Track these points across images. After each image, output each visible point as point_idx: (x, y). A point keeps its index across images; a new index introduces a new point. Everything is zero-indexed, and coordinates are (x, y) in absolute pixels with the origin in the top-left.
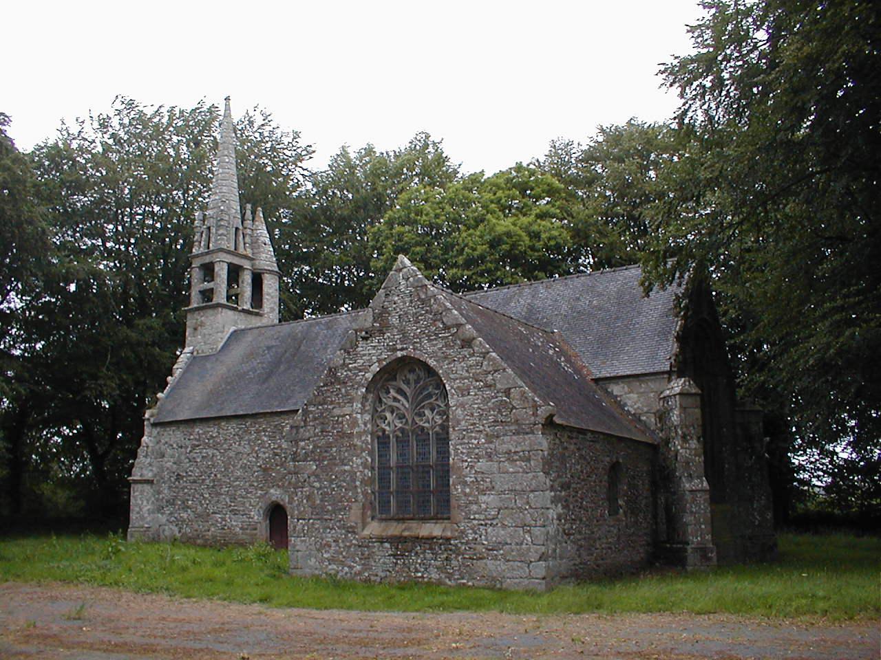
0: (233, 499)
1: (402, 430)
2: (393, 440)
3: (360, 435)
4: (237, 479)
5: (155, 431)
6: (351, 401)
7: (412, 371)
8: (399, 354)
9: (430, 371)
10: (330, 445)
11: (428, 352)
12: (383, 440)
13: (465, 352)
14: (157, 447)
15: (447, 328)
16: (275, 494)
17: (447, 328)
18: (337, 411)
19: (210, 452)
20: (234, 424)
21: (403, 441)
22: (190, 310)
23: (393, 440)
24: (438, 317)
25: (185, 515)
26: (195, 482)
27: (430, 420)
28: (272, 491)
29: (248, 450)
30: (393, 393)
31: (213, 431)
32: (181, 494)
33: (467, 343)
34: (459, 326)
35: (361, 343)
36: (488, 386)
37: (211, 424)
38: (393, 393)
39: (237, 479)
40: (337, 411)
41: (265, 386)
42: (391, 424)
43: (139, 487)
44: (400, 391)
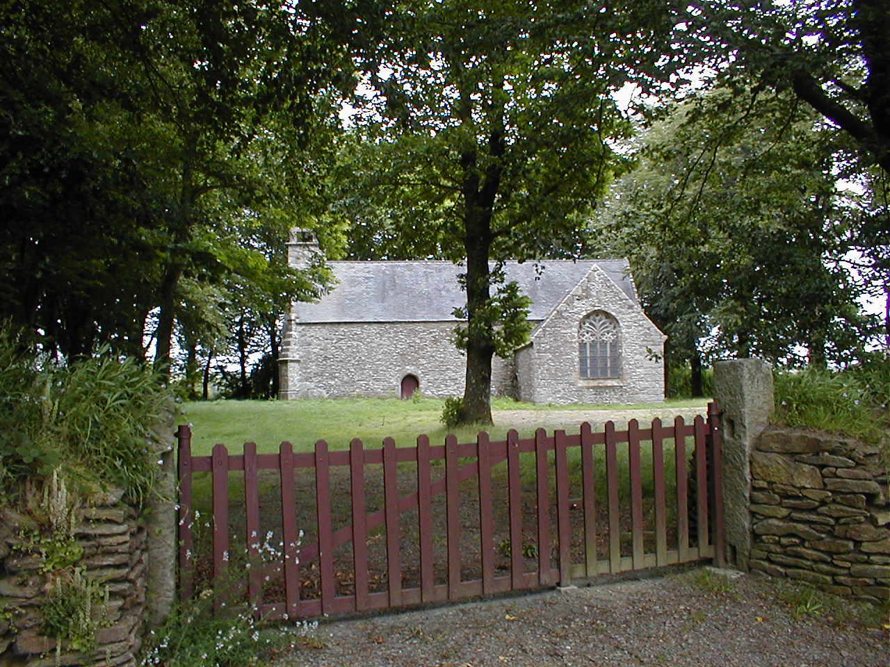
0: (376, 372)
1: (593, 341)
2: (588, 345)
3: (575, 343)
4: (379, 360)
5: (300, 328)
6: (571, 327)
7: (597, 316)
8: (596, 308)
9: (607, 315)
10: (560, 346)
11: (612, 309)
12: (582, 345)
13: (630, 311)
14: (303, 338)
15: (621, 300)
16: (410, 369)
17: (621, 300)
18: (563, 331)
19: (355, 343)
20: (375, 326)
21: (593, 344)
22: (291, 245)
23: (588, 345)
24: (616, 294)
25: (333, 383)
26: (341, 361)
27: (609, 338)
28: (408, 367)
29: (388, 342)
30: (587, 324)
31: (357, 330)
32: (329, 369)
33: (631, 307)
34: (626, 299)
35: (577, 301)
36: (640, 326)
37: (355, 325)
38: (587, 324)
39: (379, 360)
40: (563, 331)
41: (386, 304)
42: (587, 338)
43: (292, 364)
44: (591, 324)
